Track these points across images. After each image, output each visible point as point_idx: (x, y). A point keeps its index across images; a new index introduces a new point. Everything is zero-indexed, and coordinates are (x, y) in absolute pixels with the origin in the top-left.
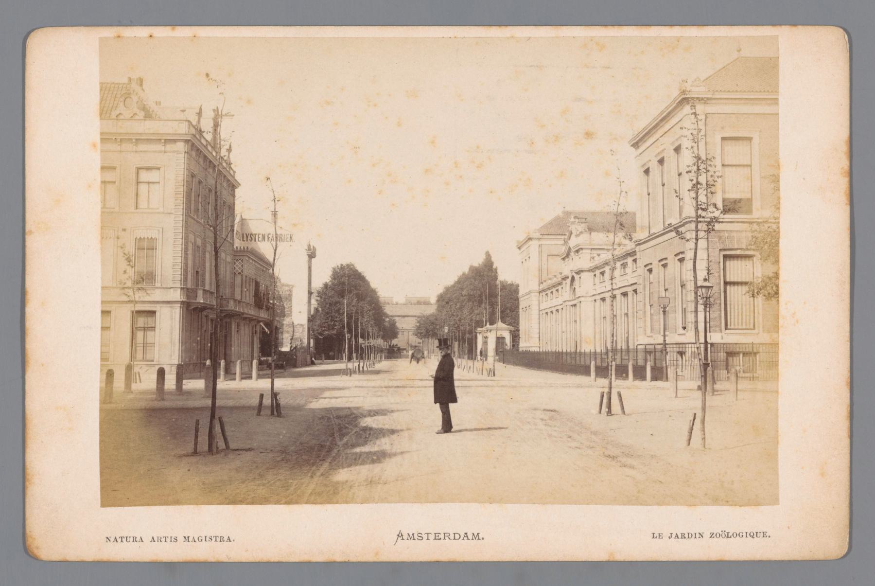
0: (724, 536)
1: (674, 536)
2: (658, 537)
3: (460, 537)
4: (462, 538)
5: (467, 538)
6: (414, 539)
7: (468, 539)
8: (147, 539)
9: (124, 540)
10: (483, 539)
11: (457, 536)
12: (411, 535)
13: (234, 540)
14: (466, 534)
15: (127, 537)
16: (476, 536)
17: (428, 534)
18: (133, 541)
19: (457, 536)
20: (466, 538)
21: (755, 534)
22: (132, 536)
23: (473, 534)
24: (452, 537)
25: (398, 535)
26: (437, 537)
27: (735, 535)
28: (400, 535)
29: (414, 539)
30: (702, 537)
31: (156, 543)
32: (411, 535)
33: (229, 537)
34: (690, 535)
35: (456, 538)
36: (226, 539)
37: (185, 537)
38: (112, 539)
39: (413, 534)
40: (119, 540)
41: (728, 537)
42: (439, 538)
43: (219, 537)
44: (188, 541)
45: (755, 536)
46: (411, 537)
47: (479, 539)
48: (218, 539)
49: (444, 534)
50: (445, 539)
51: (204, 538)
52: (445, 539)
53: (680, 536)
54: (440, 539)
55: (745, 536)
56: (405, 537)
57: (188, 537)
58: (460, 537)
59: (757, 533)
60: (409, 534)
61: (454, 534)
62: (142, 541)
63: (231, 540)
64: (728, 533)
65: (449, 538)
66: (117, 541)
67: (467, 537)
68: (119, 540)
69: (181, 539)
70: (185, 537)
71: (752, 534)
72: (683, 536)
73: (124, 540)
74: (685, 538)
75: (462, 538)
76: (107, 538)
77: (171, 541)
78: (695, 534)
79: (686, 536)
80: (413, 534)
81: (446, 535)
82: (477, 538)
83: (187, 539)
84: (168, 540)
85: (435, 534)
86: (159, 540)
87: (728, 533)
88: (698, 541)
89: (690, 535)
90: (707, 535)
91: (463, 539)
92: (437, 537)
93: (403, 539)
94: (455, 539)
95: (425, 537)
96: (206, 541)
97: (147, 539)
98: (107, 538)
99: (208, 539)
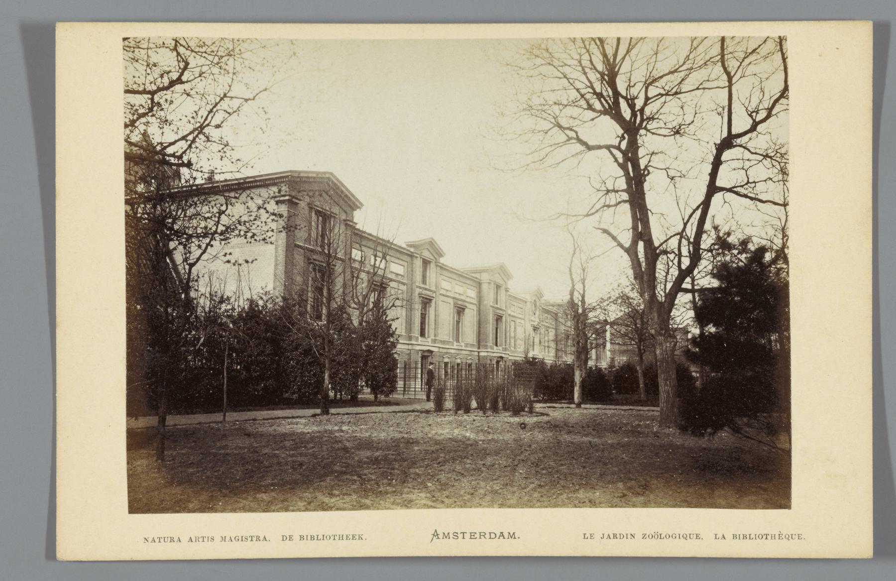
0: (656, 536)
1: (606, 536)
2: (589, 537)
4: (498, 536)
7: (504, 538)
8: (185, 539)
9: (162, 540)
10: (519, 538)
11: (493, 536)
12: (446, 534)
13: (519, 538)
14: (502, 533)
15: (164, 538)
16: (512, 536)
17: (463, 533)
18: (744, 539)
19: (493, 536)
20: (502, 538)
21: (688, 536)
23: (509, 533)
24: (488, 536)
25: (434, 535)
26: (472, 536)
27: (668, 536)
28: (436, 534)
30: (634, 537)
31: (194, 543)
32: (446, 534)
34: (622, 536)
36: (261, 538)
38: (150, 540)
39: (448, 533)
40: (157, 540)
41: (661, 538)
45: (688, 537)
46: (446, 536)
47: (515, 538)
48: (254, 539)
49: (480, 533)
50: (480, 538)
52: (480, 538)
53: (612, 536)
54: (476, 538)
55: (678, 537)
56: (441, 536)
59: (690, 534)
61: (490, 533)
64: (661, 535)
66: (155, 542)
67: (503, 536)
68: (157, 540)
69: (218, 539)
71: (685, 536)
72: (615, 536)
73: (162, 540)
74: (617, 538)
75: (498, 536)
76: (145, 539)
78: (627, 534)
79: (618, 536)
80: (448, 533)
81: (482, 534)
83: (224, 539)
86: (197, 539)
87: (661, 535)
88: (631, 541)
89: (622, 537)
90: (639, 536)
92: (472, 536)
93: (438, 538)
94: (490, 538)
95: (461, 536)
96: (242, 540)
97: (185, 539)
98: (145, 539)
99: (244, 539)
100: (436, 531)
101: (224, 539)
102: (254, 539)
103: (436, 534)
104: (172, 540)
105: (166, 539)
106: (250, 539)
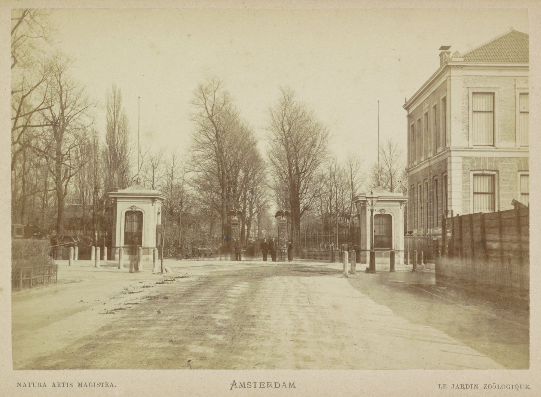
9: (32, 385)
22: (38, 382)
33: (112, 383)
37: (79, 383)
38: (22, 384)
43: (105, 384)
44: (82, 387)
48: (104, 385)
51: (93, 384)
57: (81, 383)
62: (46, 386)
63: (114, 385)
69: (76, 385)
70: (79, 383)
73: (32, 385)
77: (67, 387)
84: (65, 385)
101: (80, 385)
102: (104, 385)
104: (39, 385)
105: (35, 384)
106: (101, 385)
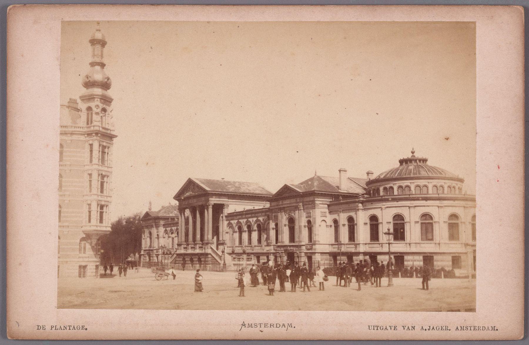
3: (280, 326)
5: (284, 326)
6: (252, 327)
11: (278, 326)
12: (250, 325)
17: (261, 324)
19: (278, 326)
24: (275, 326)
25: (242, 325)
29: (252, 327)
32: (250, 325)
35: (277, 327)
39: (251, 324)
42: (267, 326)
50: (270, 327)
52: (270, 327)
56: (247, 326)
58: (280, 326)
60: (249, 324)
65: (273, 327)
67: (284, 326)
75: (281, 325)
80: (251, 324)
82: (291, 326)
85: (265, 324)
91: (282, 327)
93: (245, 327)
94: (276, 327)
100: (244, 322)
103: (244, 325)
